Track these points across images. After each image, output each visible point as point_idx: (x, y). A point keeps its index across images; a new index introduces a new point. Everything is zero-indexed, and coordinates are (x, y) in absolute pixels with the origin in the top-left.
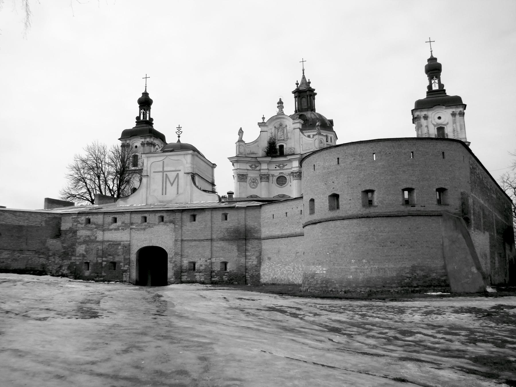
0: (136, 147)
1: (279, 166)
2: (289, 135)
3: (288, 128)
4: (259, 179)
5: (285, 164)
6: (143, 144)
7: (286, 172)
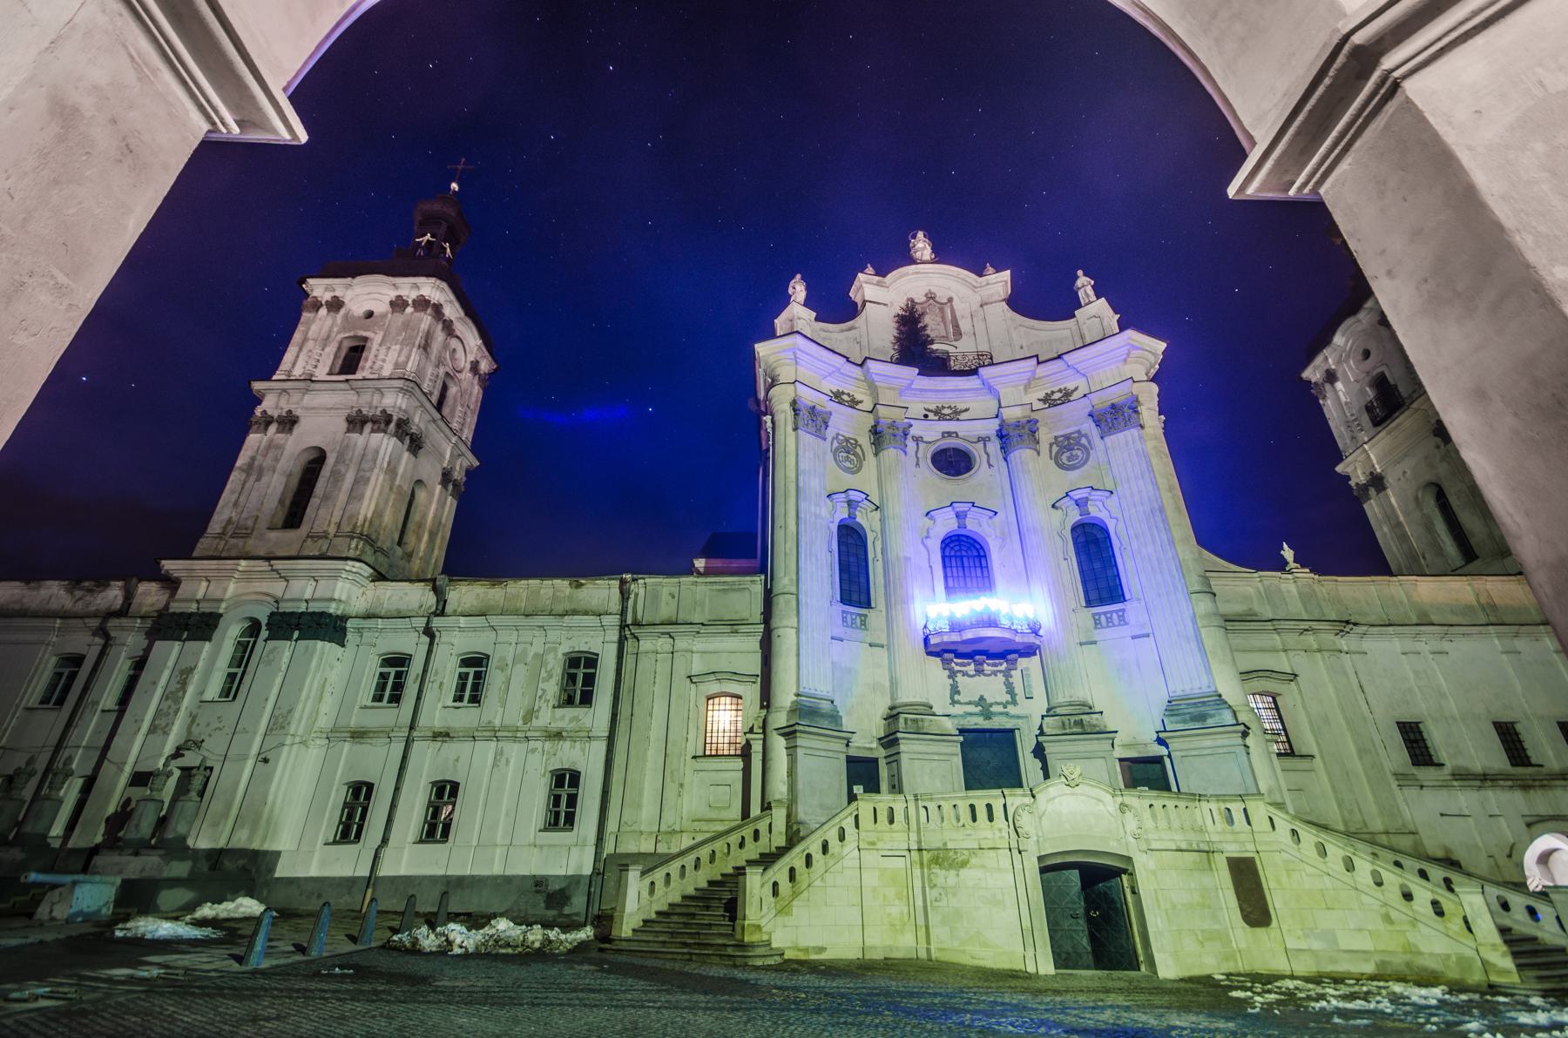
0: (370, 315)
1: (936, 412)
2: (965, 325)
4: (865, 440)
5: (961, 407)
6: (398, 304)
7: (967, 430)
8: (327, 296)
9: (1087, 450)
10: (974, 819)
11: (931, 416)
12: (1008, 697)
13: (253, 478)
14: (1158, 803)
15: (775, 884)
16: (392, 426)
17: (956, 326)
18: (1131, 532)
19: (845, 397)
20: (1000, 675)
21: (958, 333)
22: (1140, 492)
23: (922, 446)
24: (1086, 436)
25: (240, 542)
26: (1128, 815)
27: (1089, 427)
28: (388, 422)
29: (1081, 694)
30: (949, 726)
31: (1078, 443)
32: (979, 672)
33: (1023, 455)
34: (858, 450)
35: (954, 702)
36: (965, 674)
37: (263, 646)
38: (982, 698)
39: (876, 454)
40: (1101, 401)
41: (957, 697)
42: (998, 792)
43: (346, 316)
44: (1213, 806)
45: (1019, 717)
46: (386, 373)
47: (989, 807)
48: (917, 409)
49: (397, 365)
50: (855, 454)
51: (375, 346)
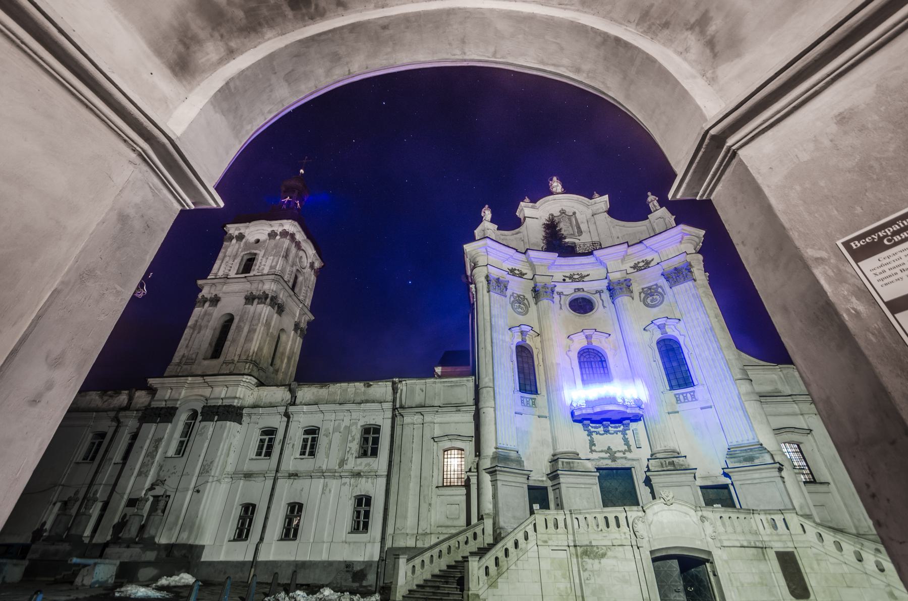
0: (258, 241)
1: (570, 277)
2: (584, 227)
3: (578, 215)
4: (529, 296)
5: (585, 273)
6: (272, 235)
7: (589, 287)
8: (237, 233)
9: (662, 295)
10: (608, 526)
11: (567, 280)
12: (626, 447)
13: (196, 332)
14: (726, 516)
15: (487, 568)
16: (268, 300)
17: (579, 228)
18: (694, 344)
19: (517, 272)
20: (619, 434)
21: (580, 232)
22: (697, 319)
23: (563, 297)
24: (661, 287)
25: (188, 367)
26: (707, 523)
27: (662, 282)
28: (266, 298)
29: (672, 445)
30: (590, 466)
31: (656, 291)
32: (607, 432)
33: (623, 300)
34: (526, 301)
35: (592, 451)
36: (598, 433)
37: (199, 425)
38: (609, 448)
39: (536, 304)
40: (668, 266)
41: (593, 448)
42: (621, 509)
43: (245, 243)
44: (763, 517)
45: (633, 460)
46: (265, 272)
47: (617, 518)
48: (558, 276)
49: (271, 267)
50: (524, 304)
51: (260, 258)
